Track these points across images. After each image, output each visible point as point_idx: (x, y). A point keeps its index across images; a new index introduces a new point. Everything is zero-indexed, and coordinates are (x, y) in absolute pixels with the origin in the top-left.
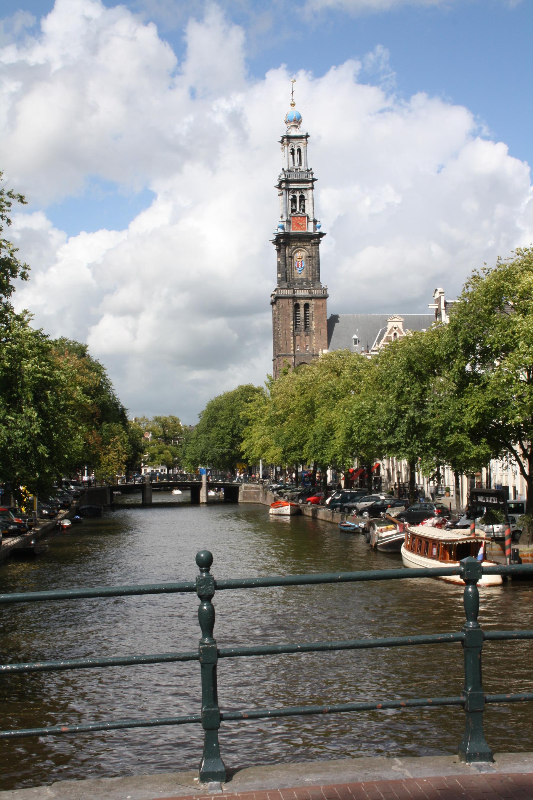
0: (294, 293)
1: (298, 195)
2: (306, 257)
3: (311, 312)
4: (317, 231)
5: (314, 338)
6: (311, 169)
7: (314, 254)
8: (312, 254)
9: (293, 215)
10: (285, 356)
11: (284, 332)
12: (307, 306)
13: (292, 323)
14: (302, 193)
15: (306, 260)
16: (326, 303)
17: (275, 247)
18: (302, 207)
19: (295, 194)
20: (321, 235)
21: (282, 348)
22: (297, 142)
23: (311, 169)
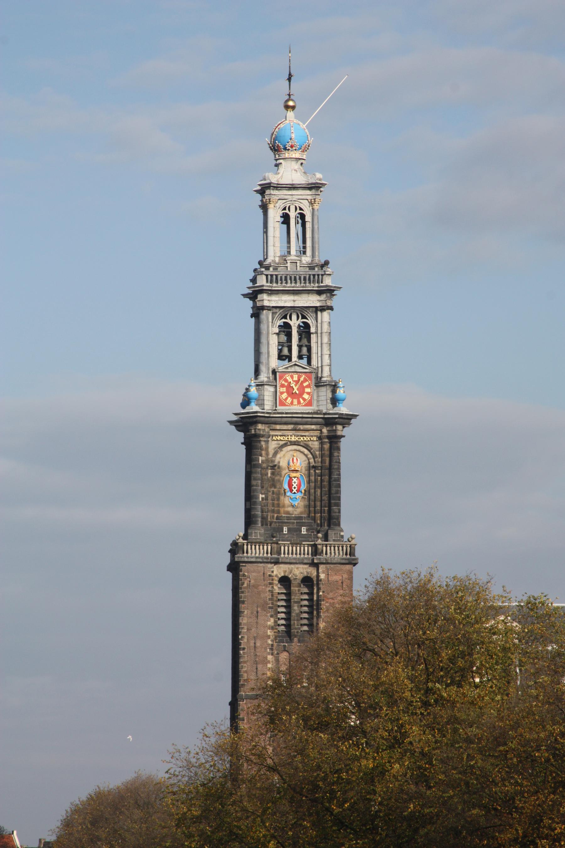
0: (279, 553)
1: (295, 322)
4: (336, 410)
11: (252, 644)
15: (309, 475)
16: (351, 579)
18: (305, 350)
19: (288, 320)
20: (346, 420)
21: (247, 680)
22: (295, 198)
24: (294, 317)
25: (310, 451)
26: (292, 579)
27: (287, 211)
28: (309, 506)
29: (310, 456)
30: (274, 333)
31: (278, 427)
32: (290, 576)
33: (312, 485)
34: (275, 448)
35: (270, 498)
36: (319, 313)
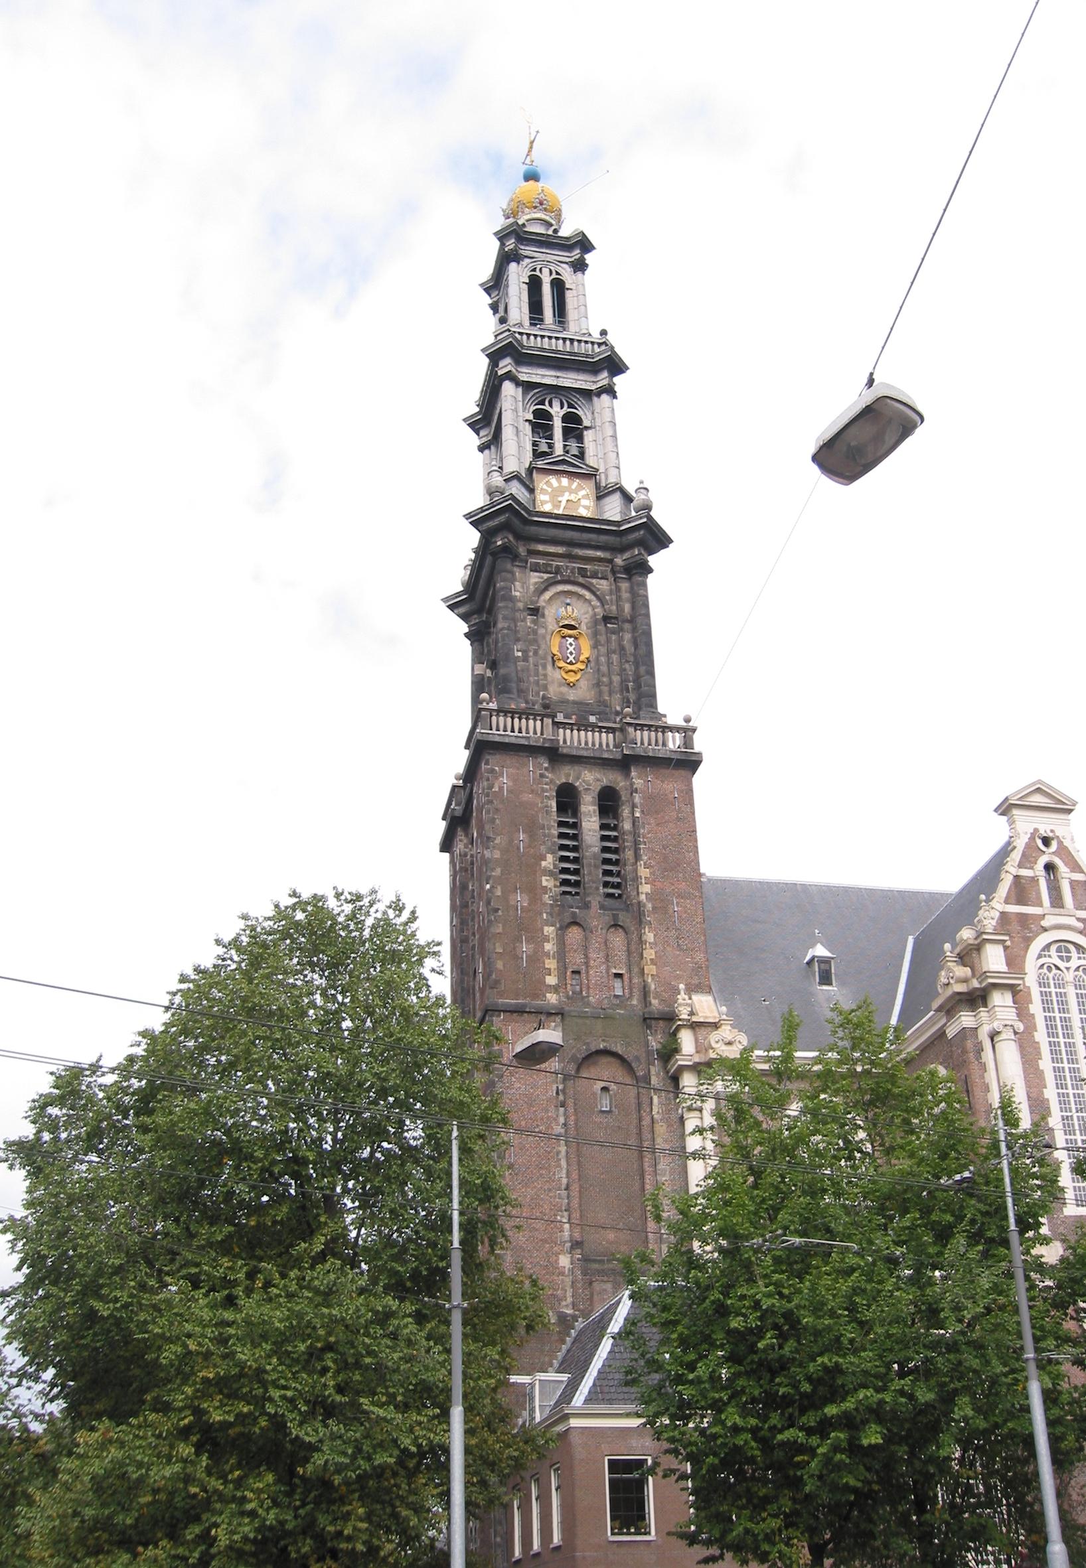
1: (557, 411)
2: (595, 622)
3: (627, 826)
5: (649, 937)
6: (604, 333)
7: (627, 607)
8: (620, 609)
9: (540, 464)
10: (519, 1011)
12: (609, 802)
13: (549, 862)
14: (570, 406)
15: (595, 634)
17: (473, 537)
19: (547, 407)
23: (604, 333)
24: (556, 404)
25: (594, 593)
26: (581, 789)
27: (538, 273)
28: (598, 684)
29: (595, 603)
30: (527, 420)
31: (541, 548)
32: (577, 784)
33: (603, 650)
34: (536, 583)
35: (531, 660)
36: (595, 399)
